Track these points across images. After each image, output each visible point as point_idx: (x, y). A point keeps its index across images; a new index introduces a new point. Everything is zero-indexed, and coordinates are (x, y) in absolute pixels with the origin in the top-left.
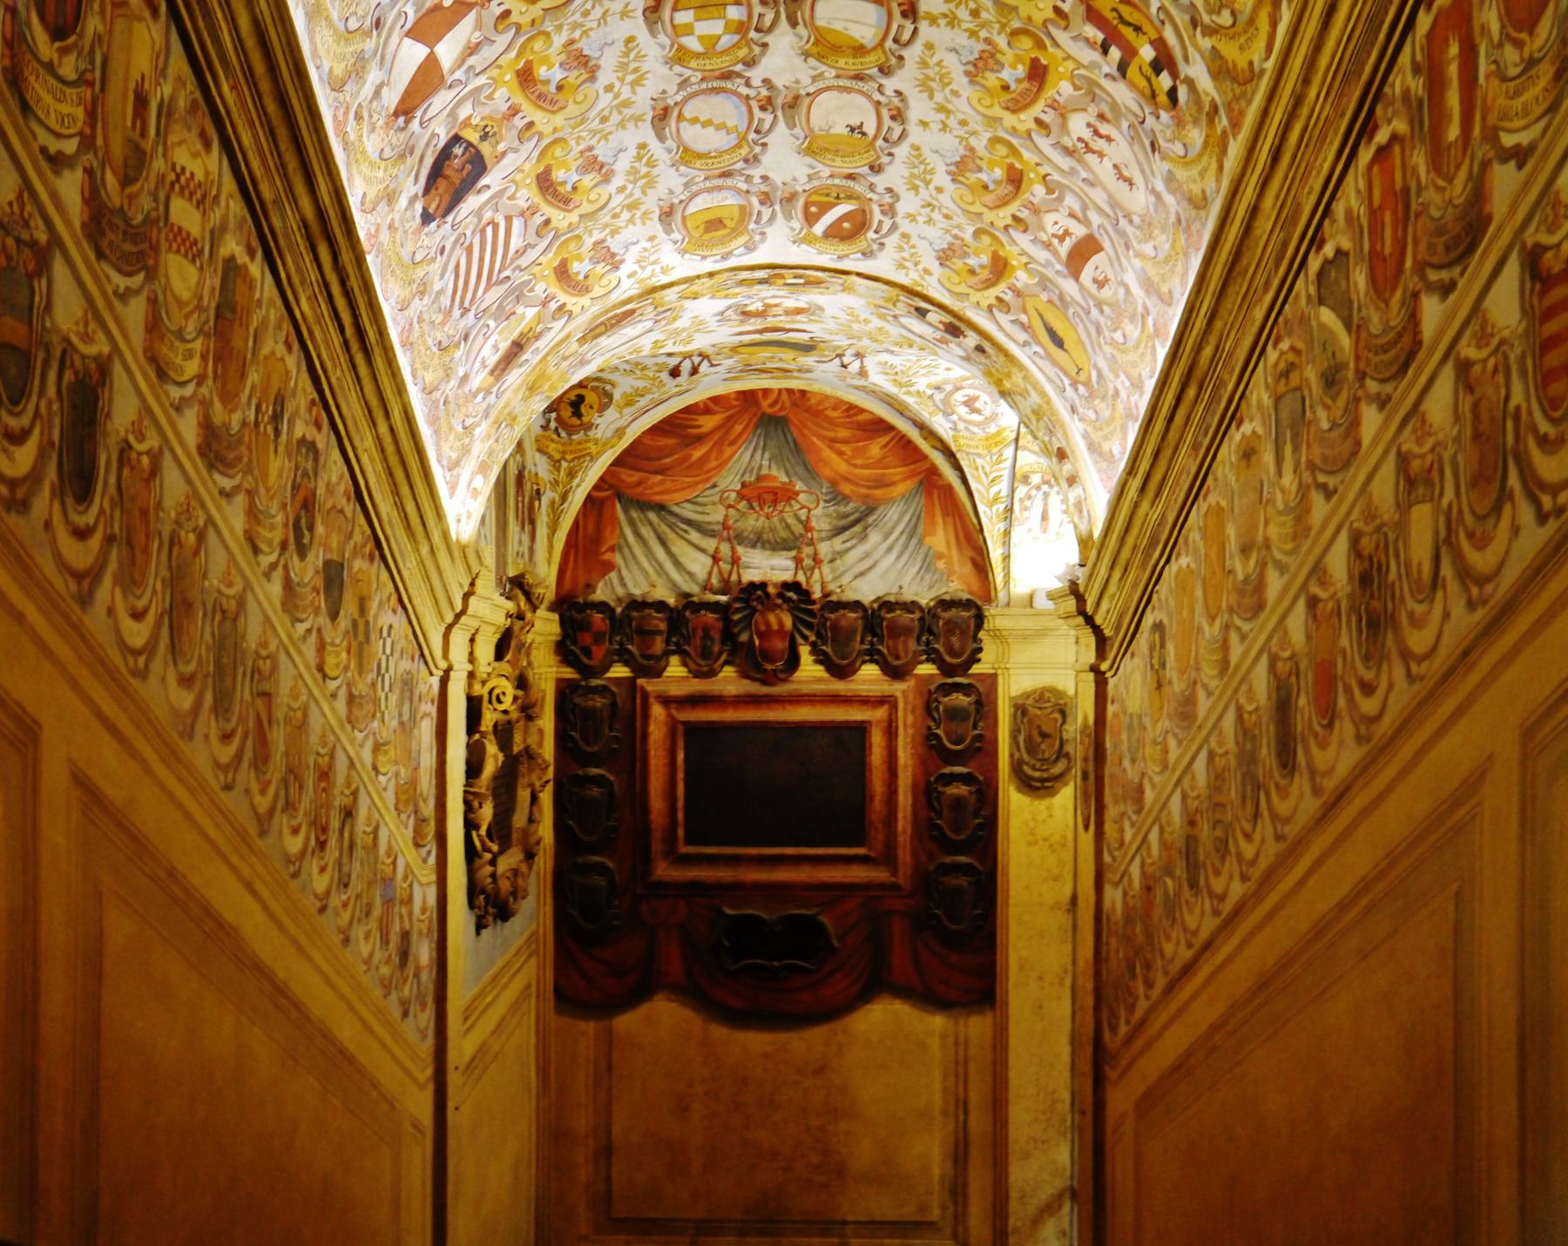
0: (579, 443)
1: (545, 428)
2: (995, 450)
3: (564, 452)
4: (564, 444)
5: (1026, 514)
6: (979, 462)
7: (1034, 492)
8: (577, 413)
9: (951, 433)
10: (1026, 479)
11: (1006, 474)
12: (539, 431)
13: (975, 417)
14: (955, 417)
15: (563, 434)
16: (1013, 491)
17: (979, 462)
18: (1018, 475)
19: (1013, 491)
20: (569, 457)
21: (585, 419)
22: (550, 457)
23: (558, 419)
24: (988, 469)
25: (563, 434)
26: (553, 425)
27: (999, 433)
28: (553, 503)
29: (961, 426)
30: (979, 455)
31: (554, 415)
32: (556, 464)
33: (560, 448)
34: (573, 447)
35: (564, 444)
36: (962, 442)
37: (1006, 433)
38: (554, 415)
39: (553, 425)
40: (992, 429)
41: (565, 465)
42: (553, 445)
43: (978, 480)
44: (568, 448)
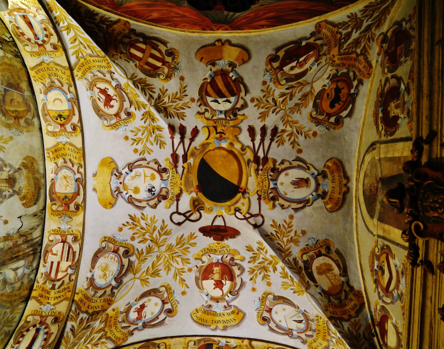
0: (344, 65)
1: (361, 82)
2: (82, 60)
3: (356, 60)
4: (353, 66)
5: (43, 26)
6: (89, 52)
7: (46, 39)
8: (338, 90)
9: (113, 70)
10: (55, 47)
11: (69, 45)
12: (365, 81)
13: (102, 86)
14: (114, 84)
15: (351, 74)
16: (60, 39)
17: (89, 52)
18: (61, 50)
19: (60, 39)
20: (354, 55)
21: (334, 86)
22: (366, 59)
23: (350, 87)
24: (82, 47)
25: (351, 74)
26: (355, 83)
27: (84, 73)
28: (378, 27)
29: (108, 77)
30: (91, 56)
31: (352, 91)
32: (365, 52)
33: (357, 64)
34: (347, 63)
35: (353, 66)
36: (104, 64)
37: (80, 74)
38: (352, 91)
39: (355, 83)
40: (89, 76)
41: (359, 51)
42: (360, 67)
43: (85, 39)
44: (352, 62)
